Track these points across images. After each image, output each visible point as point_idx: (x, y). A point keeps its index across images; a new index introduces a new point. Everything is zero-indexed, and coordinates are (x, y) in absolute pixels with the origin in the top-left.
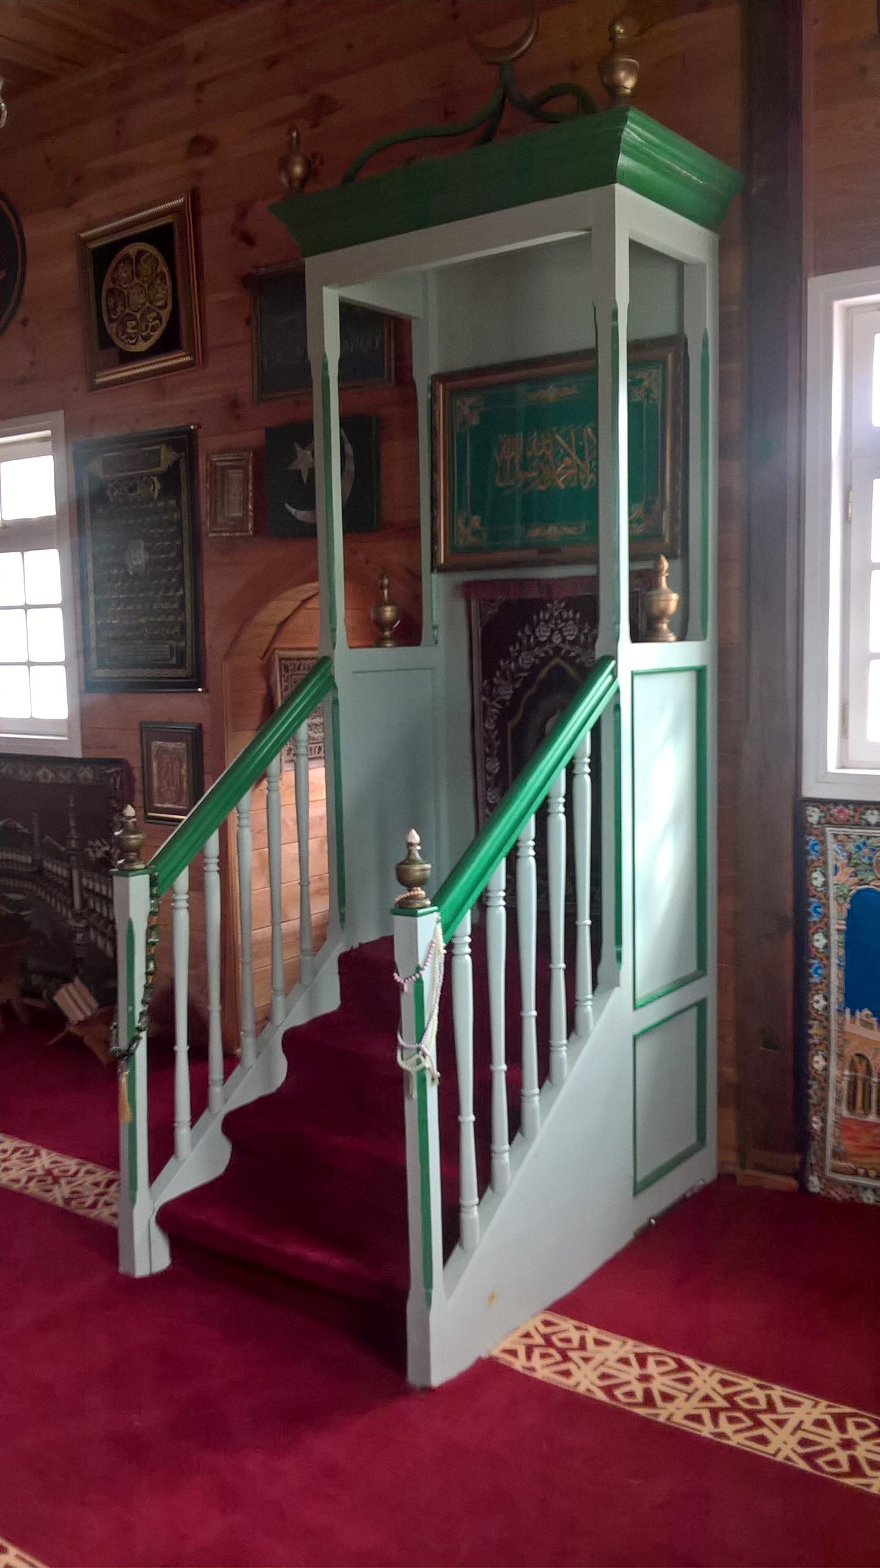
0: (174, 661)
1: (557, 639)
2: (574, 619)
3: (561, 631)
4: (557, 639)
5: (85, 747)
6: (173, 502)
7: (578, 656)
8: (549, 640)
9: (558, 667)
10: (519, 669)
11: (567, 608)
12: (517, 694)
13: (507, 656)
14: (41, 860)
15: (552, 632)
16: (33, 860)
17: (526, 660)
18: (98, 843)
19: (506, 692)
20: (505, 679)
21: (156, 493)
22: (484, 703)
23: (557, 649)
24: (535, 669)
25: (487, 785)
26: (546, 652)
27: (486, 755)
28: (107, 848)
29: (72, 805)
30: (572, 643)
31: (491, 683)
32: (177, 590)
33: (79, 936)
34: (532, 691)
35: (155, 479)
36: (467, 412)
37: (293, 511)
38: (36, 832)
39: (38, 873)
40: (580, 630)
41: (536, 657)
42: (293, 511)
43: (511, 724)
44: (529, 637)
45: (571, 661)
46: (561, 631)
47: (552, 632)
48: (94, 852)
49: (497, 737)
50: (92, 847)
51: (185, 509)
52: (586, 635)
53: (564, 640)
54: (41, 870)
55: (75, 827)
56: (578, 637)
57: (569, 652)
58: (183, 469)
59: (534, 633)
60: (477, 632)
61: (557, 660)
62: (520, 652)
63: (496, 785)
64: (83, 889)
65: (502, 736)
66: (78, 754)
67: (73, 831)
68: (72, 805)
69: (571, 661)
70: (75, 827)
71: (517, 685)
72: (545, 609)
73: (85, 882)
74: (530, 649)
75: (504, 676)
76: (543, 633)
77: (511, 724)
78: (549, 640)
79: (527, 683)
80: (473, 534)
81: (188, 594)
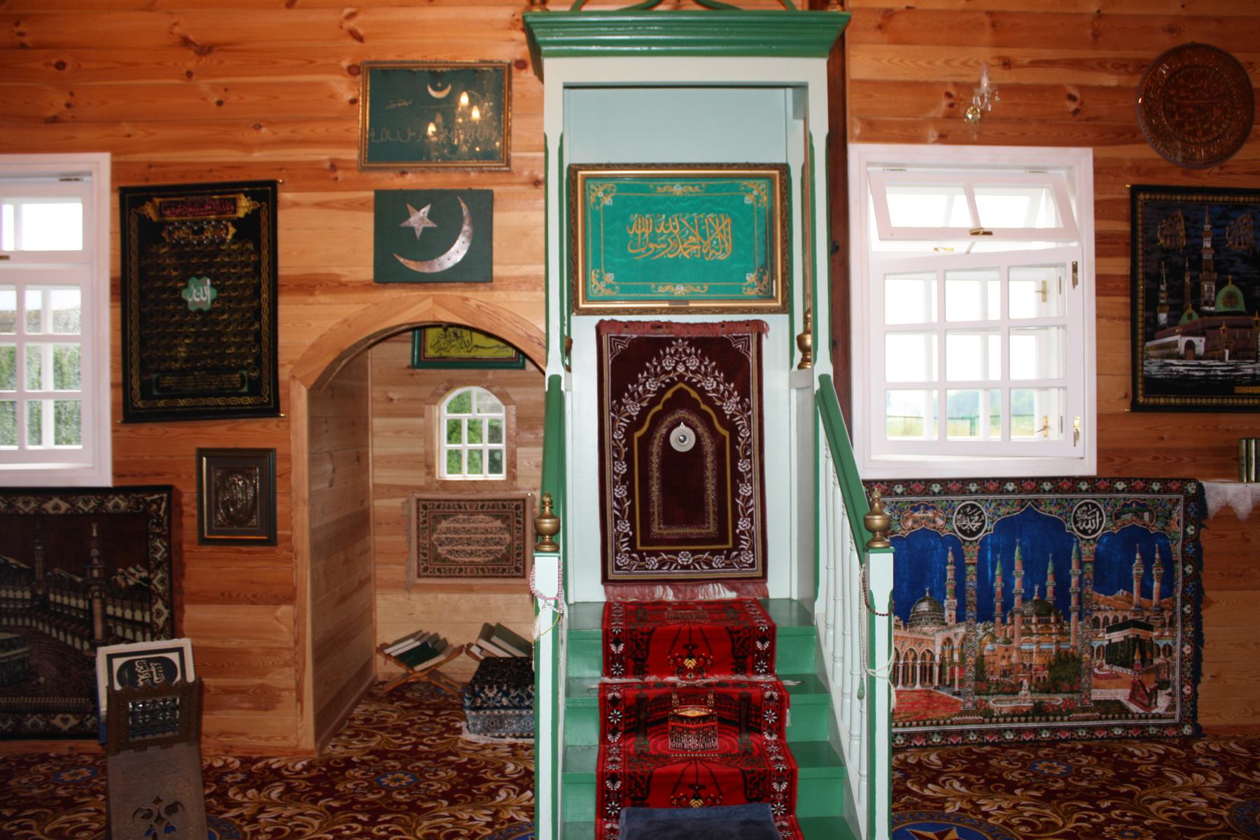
0: (245, 390)
1: (681, 369)
2: (696, 354)
3: (684, 363)
4: (681, 369)
5: (116, 474)
6: (250, 246)
7: (699, 381)
8: (674, 369)
9: (681, 389)
10: (646, 391)
11: (690, 346)
12: (644, 411)
13: (635, 381)
14: (46, 596)
15: (677, 363)
16: (34, 596)
17: (652, 385)
18: (132, 570)
19: (633, 409)
20: (633, 399)
21: (229, 237)
22: (613, 419)
23: (681, 377)
24: (660, 392)
25: (615, 483)
26: (672, 379)
27: (615, 459)
28: (144, 574)
29: (95, 534)
30: (692, 372)
31: (620, 403)
34: (659, 407)
36: (601, 194)
37: (402, 260)
38: (39, 566)
39: (41, 608)
40: (701, 363)
41: (663, 382)
42: (402, 260)
43: (637, 434)
44: (655, 367)
45: (693, 386)
46: (684, 363)
47: (677, 363)
48: (125, 579)
49: (625, 446)
50: (122, 574)
51: (265, 252)
52: (706, 367)
53: (687, 369)
54: (45, 602)
55: (98, 557)
56: (699, 367)
57: (690, 379)
58: (264, 219)
59: (660, 363)
60: (608, 362)
61: (681, 385)
62: (647, 379)
63: (623, 483)
64: (106, 617)
65: (629, 444)
66: (106, 480)
67: (95, 561)
68: (95, 534)
69: (693, 386)
70: (98, 557)
71: (645, 404)
72: (671, 346)
73: (110, 610)
74: (656, 375)
75: (632, 396)
76: (668, 364)
77: (637, 434)
78: (674, 369)
79: (653, 402)
80: (606, 288)
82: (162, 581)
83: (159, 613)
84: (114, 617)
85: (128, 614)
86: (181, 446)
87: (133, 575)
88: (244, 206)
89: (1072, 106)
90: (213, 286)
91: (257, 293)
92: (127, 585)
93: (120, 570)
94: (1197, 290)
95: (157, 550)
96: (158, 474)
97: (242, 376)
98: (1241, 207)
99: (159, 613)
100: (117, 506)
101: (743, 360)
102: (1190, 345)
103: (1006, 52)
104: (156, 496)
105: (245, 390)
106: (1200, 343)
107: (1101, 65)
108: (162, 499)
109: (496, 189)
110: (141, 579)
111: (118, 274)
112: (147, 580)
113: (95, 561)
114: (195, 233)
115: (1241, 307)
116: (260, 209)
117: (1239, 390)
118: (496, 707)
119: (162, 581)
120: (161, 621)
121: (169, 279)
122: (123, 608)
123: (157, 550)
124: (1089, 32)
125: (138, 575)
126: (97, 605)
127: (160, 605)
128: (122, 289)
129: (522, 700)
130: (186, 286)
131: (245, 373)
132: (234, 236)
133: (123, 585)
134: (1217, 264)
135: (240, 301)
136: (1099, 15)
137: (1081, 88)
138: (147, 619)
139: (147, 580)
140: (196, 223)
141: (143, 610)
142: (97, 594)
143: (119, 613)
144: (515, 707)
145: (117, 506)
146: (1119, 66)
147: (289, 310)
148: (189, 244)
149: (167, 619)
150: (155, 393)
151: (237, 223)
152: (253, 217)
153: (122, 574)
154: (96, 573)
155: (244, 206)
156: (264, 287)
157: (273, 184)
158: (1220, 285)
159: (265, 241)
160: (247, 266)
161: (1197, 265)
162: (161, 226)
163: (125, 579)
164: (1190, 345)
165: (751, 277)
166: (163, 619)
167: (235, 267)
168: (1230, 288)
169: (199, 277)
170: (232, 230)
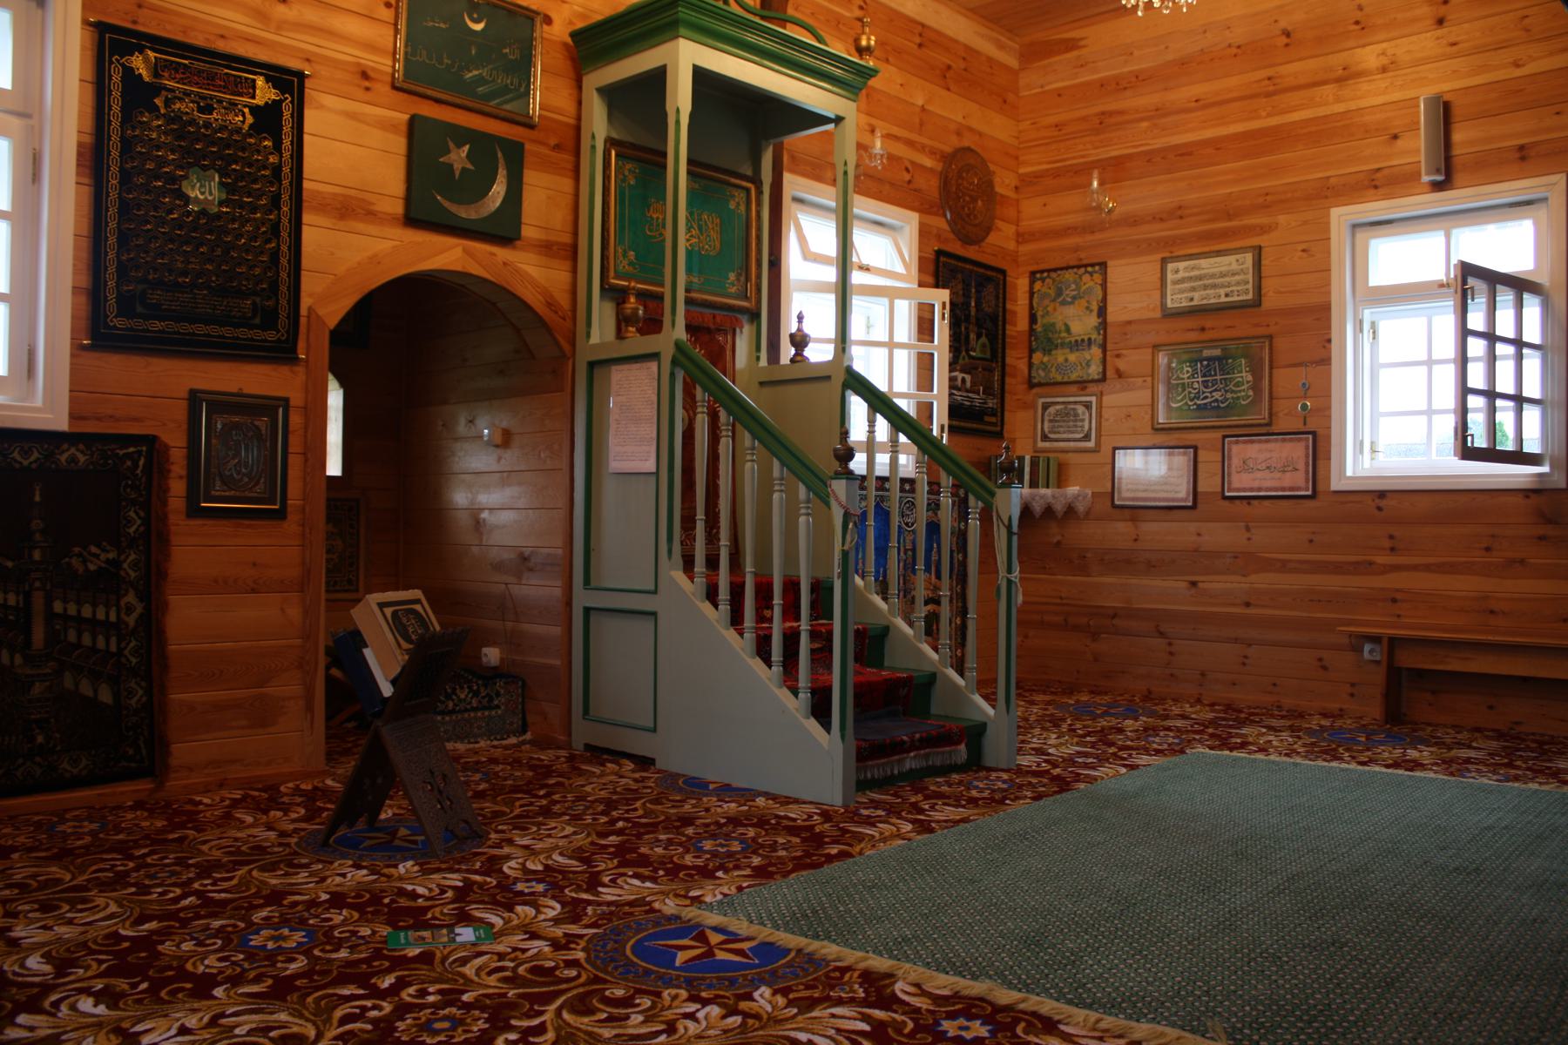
0: (257, 321)
5: (74, 417)
18: (94, 549)
28: (111, 556)
29: (37, 498)
32: (268, 241)
33: (37, 689)
35: (246, 110)
48: (85, 562)
50: (80, 555)
58: (287, 114)
64: (50, 616)
67: (38, 537)
68: (37, 498)
73: (58, 607)
81: (284, 248)
82: (134, 565)
83: (130, 609)
84: (65, 617)
85: (87, 612)
86: (158, 390)
87: (97, 556)
88: (264, 93)
89: (907, 177)
90: (221, 183)
91: (276, 202)
92: (87, 570)
93: (77, 550)
94: (967, 337)
95: (130, 522)
96: (136, 419)
97: (254, 303)
98: (989, 279)
99: (130, 609)
100: (73, 460)
101: (722, 349)
102: (963, 380)
103: (874, 122)
104: (131, 450)
105: (257, 321)
106: (968, 378)
107: (922, 149)
108: (140, 453)
109: (528, 146)
110: (107, 561)
111: (88, 139)
112: (116, 563)
113: (38, 537)
114: (201, 110)
115: (988, 356)
116: (281, 101)
117: (987, 419)
118: (466, 710)
119: (134, 565)
120: (131, 620)
121: (162, 162)
122: (79, 603)
123: (130, 522)
124: (917, 120)
125: (103, 557)
126: (38, 601)
127: (131, 598)
128: (94, 159)
129: (491, 700)
130: (185, 177)
131: (258, 300)
132: (251, 127)
133: (81, 570)
134: (977, 319)
135: (254, 209)
136: (923, 109)
137: (913, 163)
138: (113, 618)
139: (116, 563)
140: (203, 98)
141: (108, 607)
142: (37, 584)
143: (72, 610)
144: (485, 708)
145: (73, 460)
146: (932, 153)
147: (316, 235)
148: (192, 122)
149: (141, 615)
150: (139, 309)
151: (255, 110)
152: (273, 108)
153: (80, 555)
154: (37, 555)
155: (264, 93)
156: (285, 197)
157: (301, 76)
158: (979, 336)
159: (287, 142)
160: (265, 168)
161: (968, 317)
162: (156, 89)
163: (85, 562)
164: (963, 380)
165: (732, 276)
166: (135, 615)
167: (250, 165)
168: (984, 339)
169: (205, 168)
170: (250, 120)
